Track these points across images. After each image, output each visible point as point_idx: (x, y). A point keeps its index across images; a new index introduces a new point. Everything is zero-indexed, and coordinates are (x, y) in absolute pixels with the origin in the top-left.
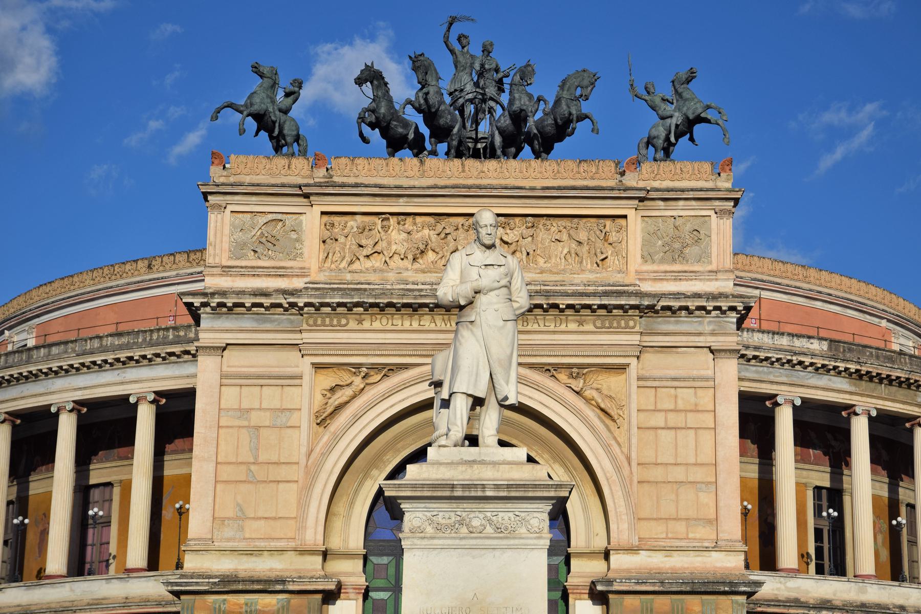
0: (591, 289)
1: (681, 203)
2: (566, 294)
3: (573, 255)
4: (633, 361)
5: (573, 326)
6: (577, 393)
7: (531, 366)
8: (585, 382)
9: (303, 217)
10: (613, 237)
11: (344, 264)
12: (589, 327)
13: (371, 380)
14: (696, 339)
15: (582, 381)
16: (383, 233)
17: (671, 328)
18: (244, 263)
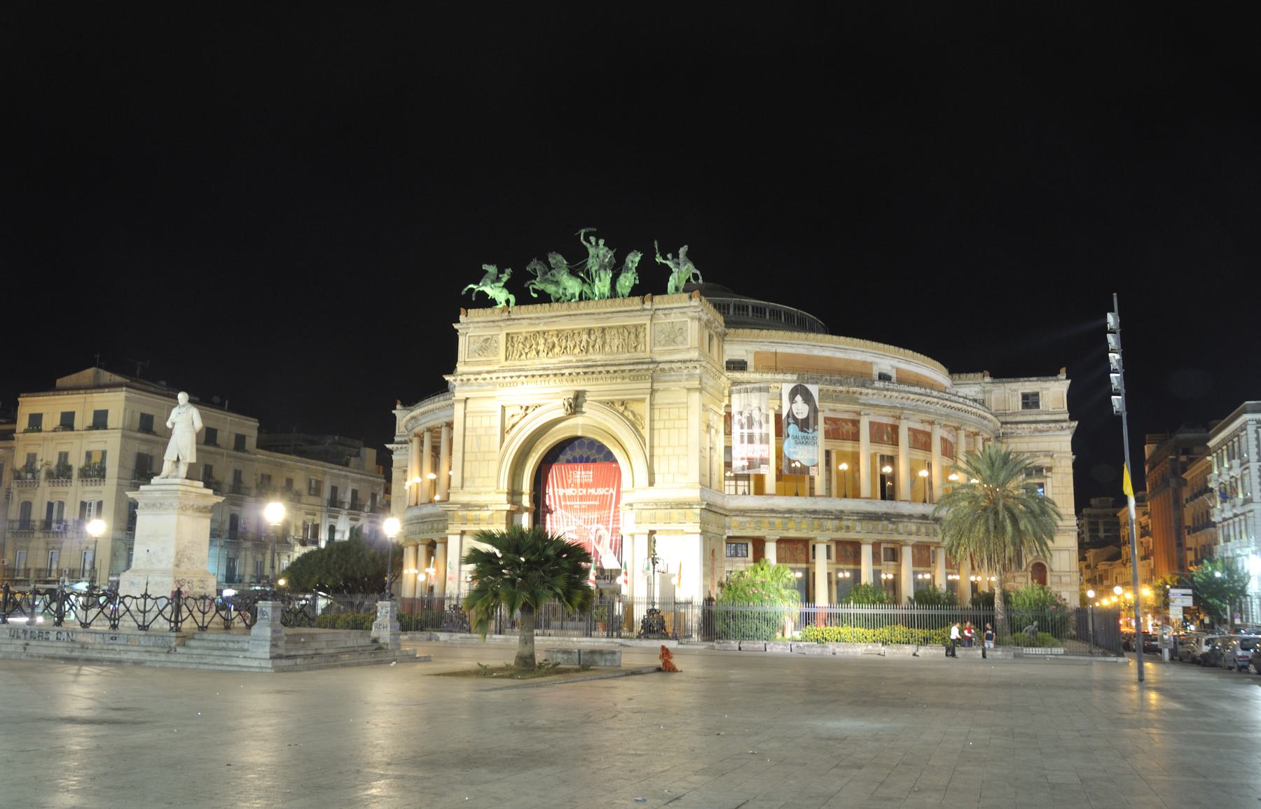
0: (628, 362)
1: (673, 315)
2: (615, 365)
3: (621, 346)
4: (648, 397)
5: (619, 380)
6: (622, 414)
7: (600, 402)
8: (626, 408)
9: (500, 336)
10: (641, 335)
11: (517, 357)
12: (627, 380)
13: (527, 412)
14: (679, 383)
15: (623, 407)
16: (533, 342)
17: (667, 378)
18: (474, 360)
